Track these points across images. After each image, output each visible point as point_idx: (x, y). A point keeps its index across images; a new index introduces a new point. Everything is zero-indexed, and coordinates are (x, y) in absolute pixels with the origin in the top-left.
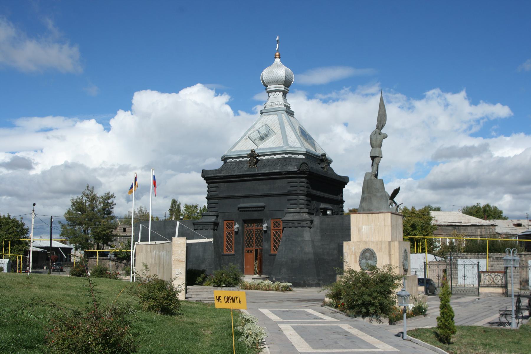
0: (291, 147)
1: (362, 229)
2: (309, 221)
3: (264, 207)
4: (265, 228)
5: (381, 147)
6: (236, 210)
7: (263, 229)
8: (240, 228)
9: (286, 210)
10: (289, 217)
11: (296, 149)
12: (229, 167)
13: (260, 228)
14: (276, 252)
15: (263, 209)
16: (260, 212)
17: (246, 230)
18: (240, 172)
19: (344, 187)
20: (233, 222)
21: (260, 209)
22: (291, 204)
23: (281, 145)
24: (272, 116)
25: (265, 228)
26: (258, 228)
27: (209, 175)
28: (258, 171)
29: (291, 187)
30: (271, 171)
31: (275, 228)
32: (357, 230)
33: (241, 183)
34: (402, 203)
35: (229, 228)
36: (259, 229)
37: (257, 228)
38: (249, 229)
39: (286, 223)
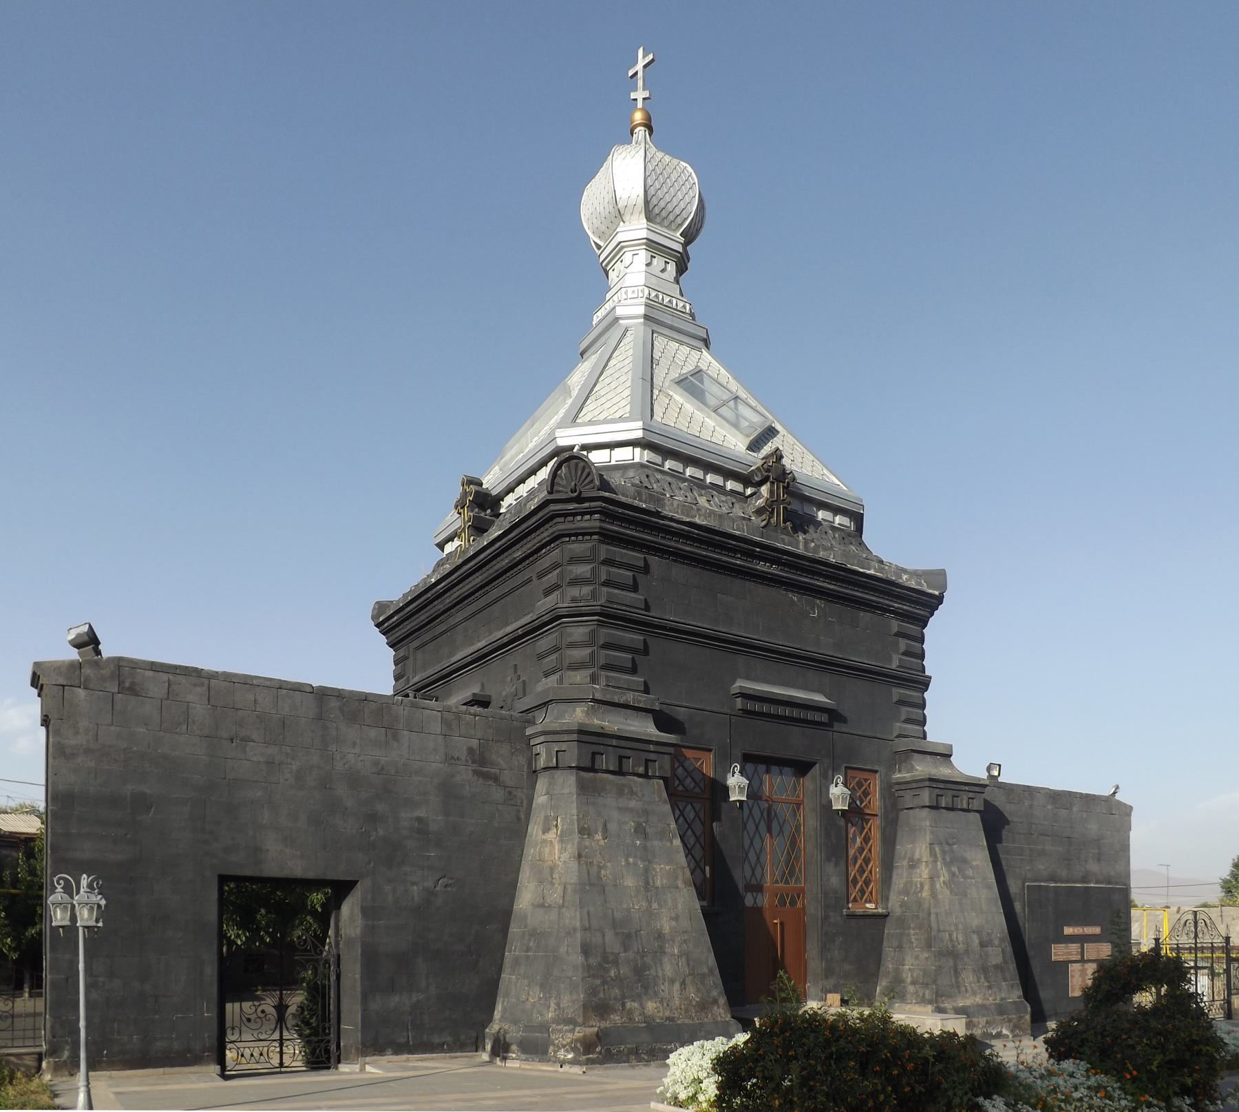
15: (824, 718)
21: (817, 717)
33: (737, 584)
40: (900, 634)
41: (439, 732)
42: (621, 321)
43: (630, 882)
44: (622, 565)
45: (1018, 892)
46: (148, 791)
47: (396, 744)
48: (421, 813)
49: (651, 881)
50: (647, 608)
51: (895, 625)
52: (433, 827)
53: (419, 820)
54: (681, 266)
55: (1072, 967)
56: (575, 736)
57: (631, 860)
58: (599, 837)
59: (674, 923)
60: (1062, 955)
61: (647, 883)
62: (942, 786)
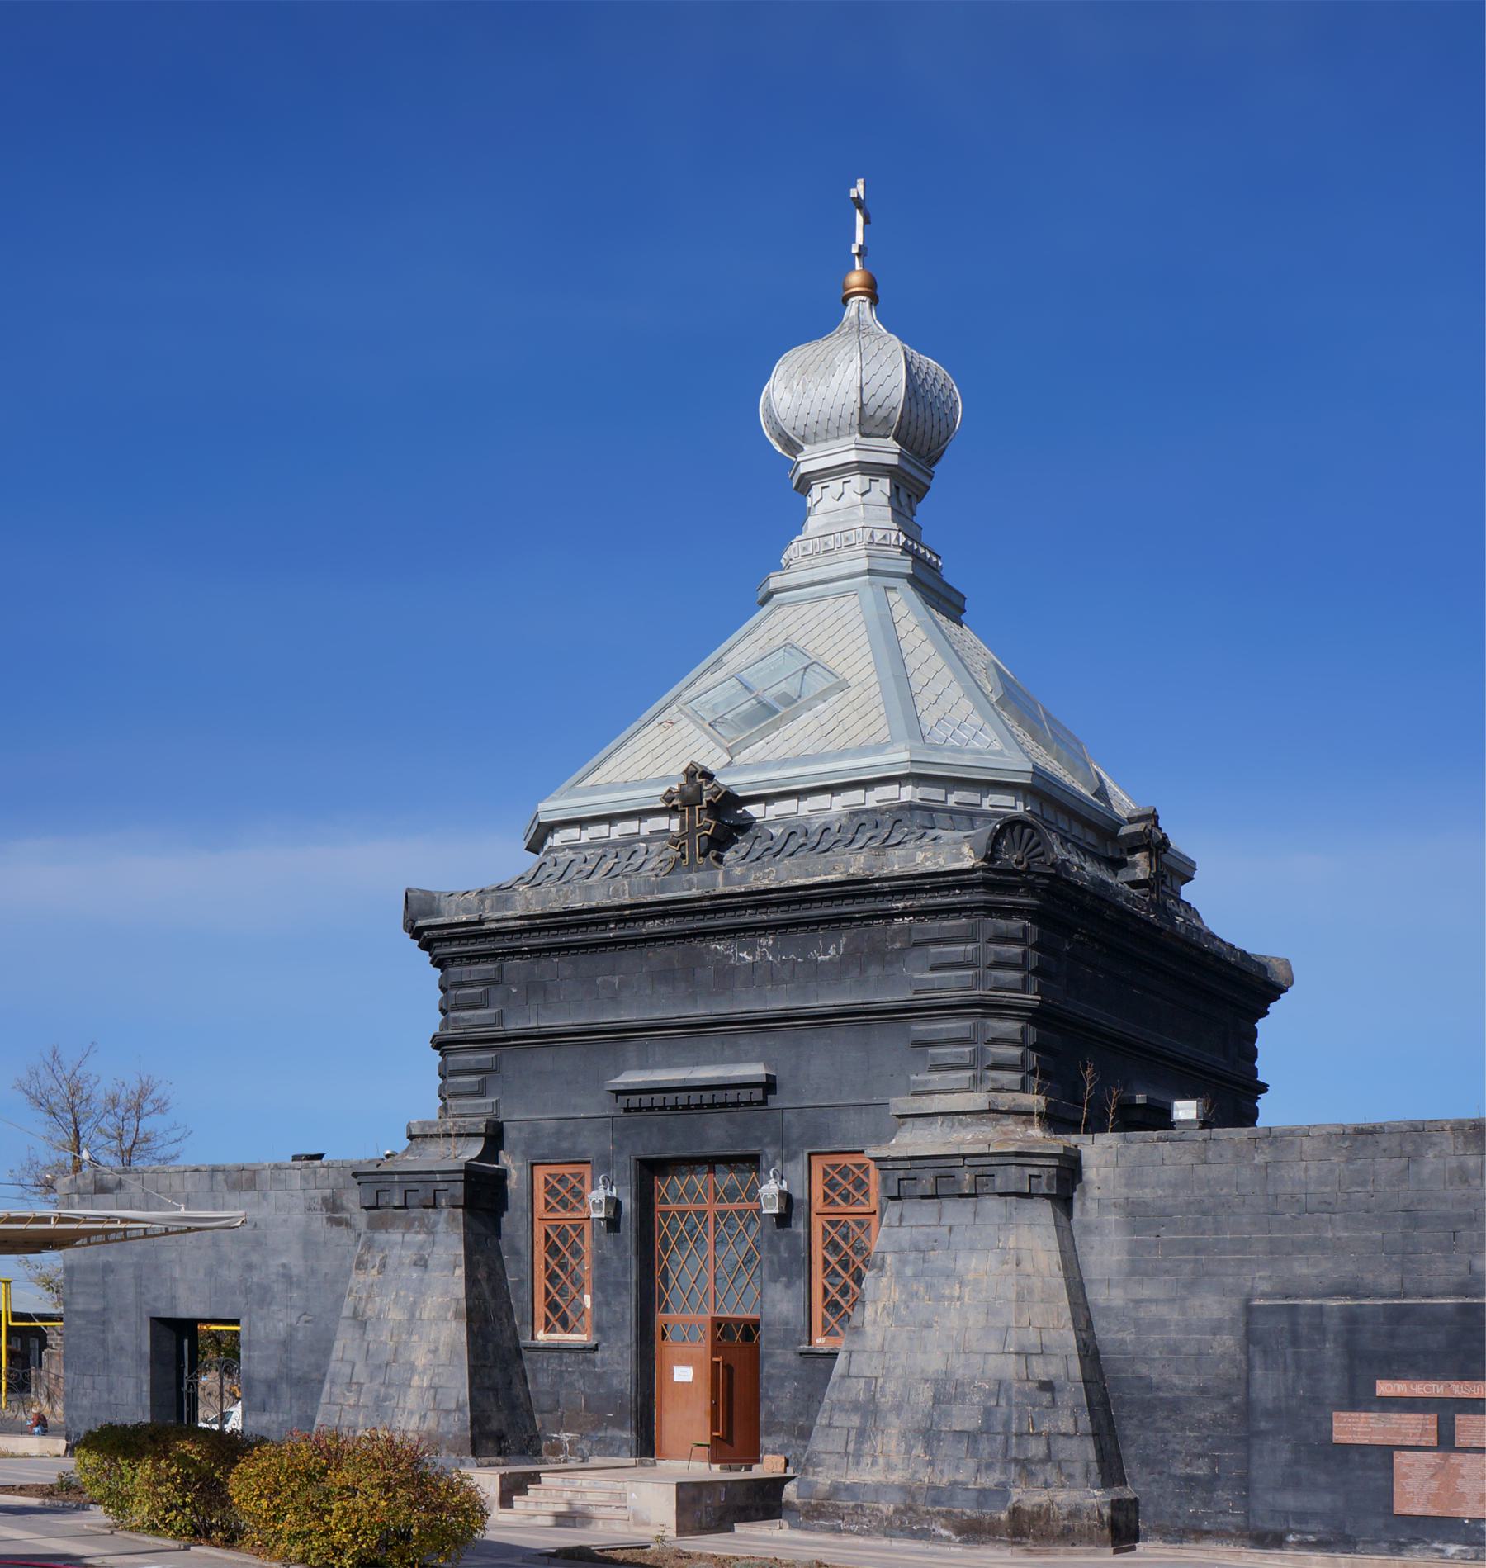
0: (935, 748)
2: (1047, 1162)
4: (770, 1202)
6: (611, 1109)
7: (758, 1211)
8: (628, 1204)
9: (902, 1104)
11: (967, 760)
13: (746, 1205)
14: (842, 1344)
17: (665, 1214)
20: (586, 1170)
22: (937, 1068)
23: (879, 737)
25: (770, 1202)
26: (736, 1205)
31: (833, 1202)
35: (564, 1204)
37: (727, 1206)
38: (682, 1214)
42: (775, 596)
43: (396, 1315)
45: (1227, 1318)
46: (111, 1260)
47: (265, 1204)
48: (284, 1260)
49: (417, 1314)
52: (295, 1271)
53: (284, 1266)
54: (878, 470)
55: (1400, 1458)
57: (402, 1293)
58: (374, 1272)
59: (430, 1356)
60: (1363, 1433)
61: (413, 1315)
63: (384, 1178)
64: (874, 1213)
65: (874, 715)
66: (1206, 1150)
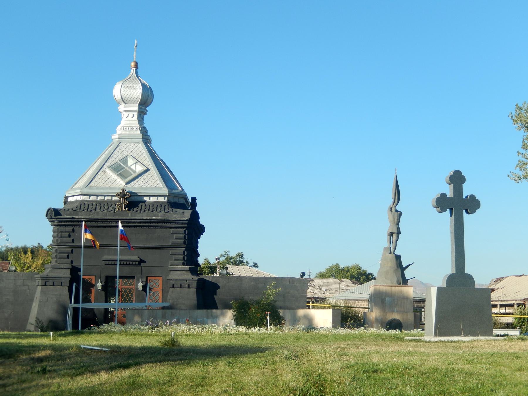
1: (385, 300)
3: (141, 262)
5: (398, 223)
10: (174, 276)
12: (86, 207)
16: (133, 267)
18: (106, 216)
19: (200, 238)
20: (93, 278)
21: (134, 263)
24: (133, 144)
27: (61, 215)
28: (131, 216)
29: (176, 239)
30: (151, 218)
32: (381, 302)
34: (415, 277)
36: (128, 288)
39: (173, 283)
40: (173, 233)
41: (13, 278)
44: (66, 232)
50: (73, 241)
51: (172, 230)
56: (40, 278)
62: (175, 281)
63: (47, 279)
64: (161, 290)
65: (156, 179)
66: (228, 280)
